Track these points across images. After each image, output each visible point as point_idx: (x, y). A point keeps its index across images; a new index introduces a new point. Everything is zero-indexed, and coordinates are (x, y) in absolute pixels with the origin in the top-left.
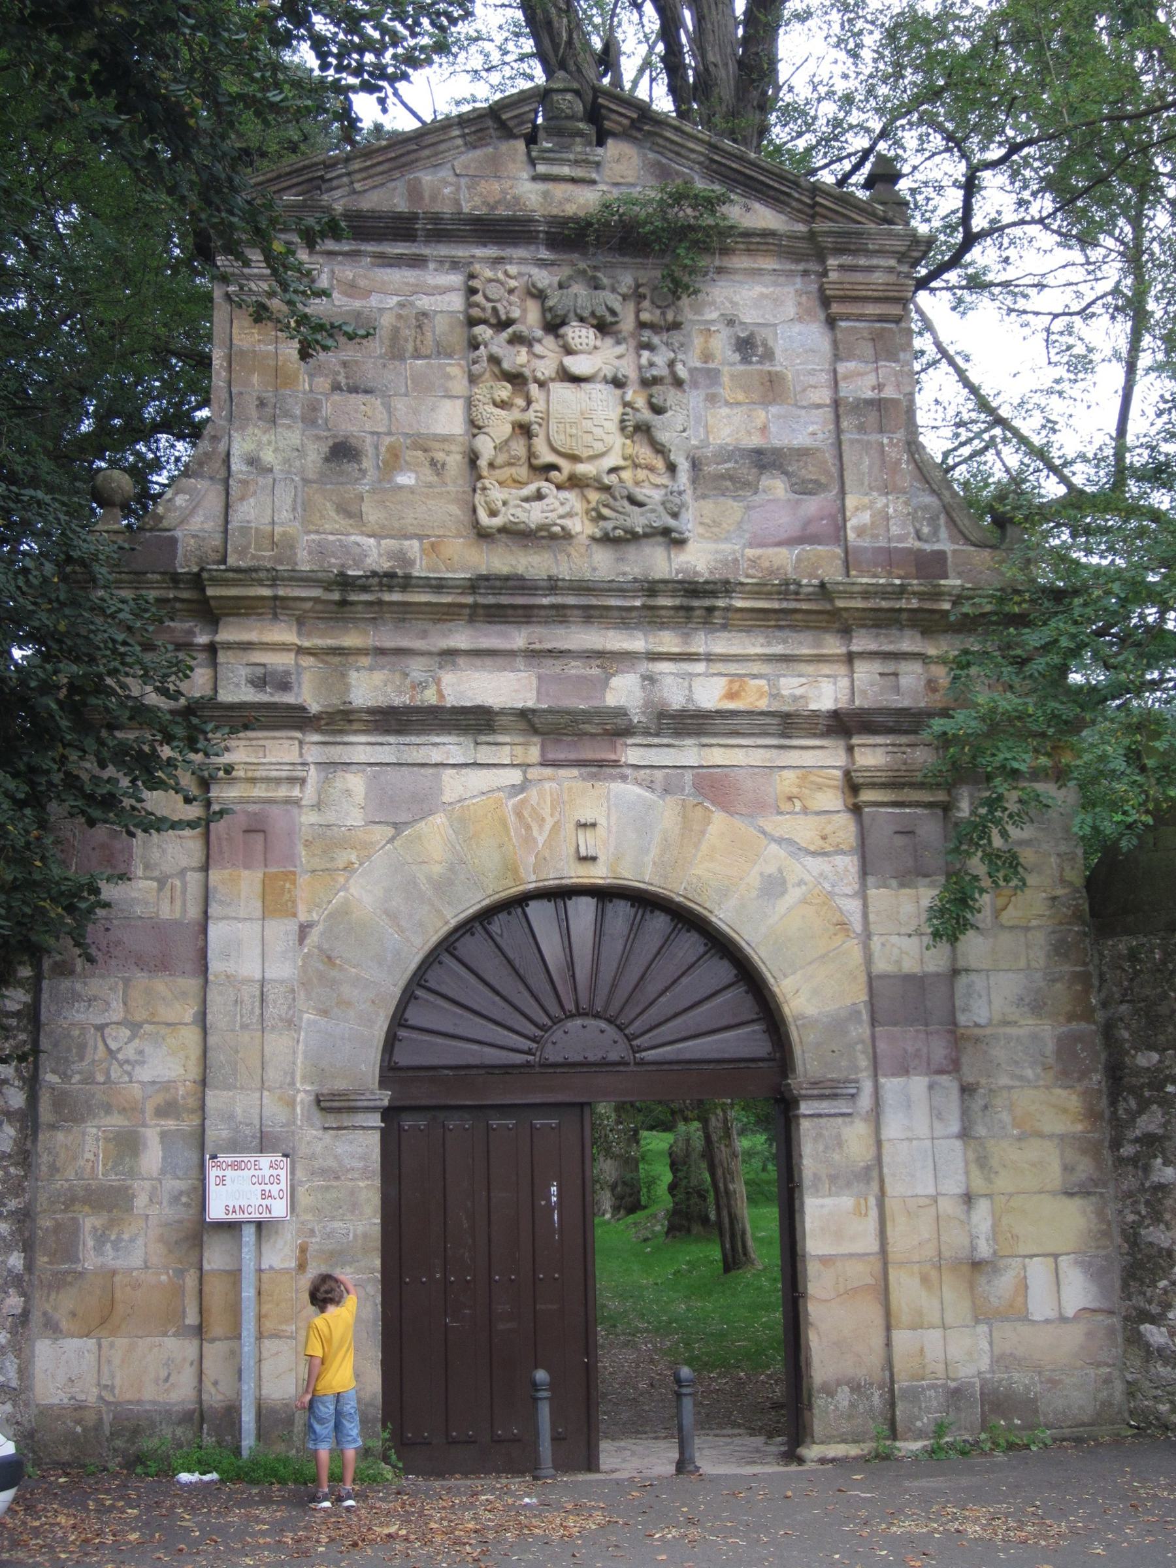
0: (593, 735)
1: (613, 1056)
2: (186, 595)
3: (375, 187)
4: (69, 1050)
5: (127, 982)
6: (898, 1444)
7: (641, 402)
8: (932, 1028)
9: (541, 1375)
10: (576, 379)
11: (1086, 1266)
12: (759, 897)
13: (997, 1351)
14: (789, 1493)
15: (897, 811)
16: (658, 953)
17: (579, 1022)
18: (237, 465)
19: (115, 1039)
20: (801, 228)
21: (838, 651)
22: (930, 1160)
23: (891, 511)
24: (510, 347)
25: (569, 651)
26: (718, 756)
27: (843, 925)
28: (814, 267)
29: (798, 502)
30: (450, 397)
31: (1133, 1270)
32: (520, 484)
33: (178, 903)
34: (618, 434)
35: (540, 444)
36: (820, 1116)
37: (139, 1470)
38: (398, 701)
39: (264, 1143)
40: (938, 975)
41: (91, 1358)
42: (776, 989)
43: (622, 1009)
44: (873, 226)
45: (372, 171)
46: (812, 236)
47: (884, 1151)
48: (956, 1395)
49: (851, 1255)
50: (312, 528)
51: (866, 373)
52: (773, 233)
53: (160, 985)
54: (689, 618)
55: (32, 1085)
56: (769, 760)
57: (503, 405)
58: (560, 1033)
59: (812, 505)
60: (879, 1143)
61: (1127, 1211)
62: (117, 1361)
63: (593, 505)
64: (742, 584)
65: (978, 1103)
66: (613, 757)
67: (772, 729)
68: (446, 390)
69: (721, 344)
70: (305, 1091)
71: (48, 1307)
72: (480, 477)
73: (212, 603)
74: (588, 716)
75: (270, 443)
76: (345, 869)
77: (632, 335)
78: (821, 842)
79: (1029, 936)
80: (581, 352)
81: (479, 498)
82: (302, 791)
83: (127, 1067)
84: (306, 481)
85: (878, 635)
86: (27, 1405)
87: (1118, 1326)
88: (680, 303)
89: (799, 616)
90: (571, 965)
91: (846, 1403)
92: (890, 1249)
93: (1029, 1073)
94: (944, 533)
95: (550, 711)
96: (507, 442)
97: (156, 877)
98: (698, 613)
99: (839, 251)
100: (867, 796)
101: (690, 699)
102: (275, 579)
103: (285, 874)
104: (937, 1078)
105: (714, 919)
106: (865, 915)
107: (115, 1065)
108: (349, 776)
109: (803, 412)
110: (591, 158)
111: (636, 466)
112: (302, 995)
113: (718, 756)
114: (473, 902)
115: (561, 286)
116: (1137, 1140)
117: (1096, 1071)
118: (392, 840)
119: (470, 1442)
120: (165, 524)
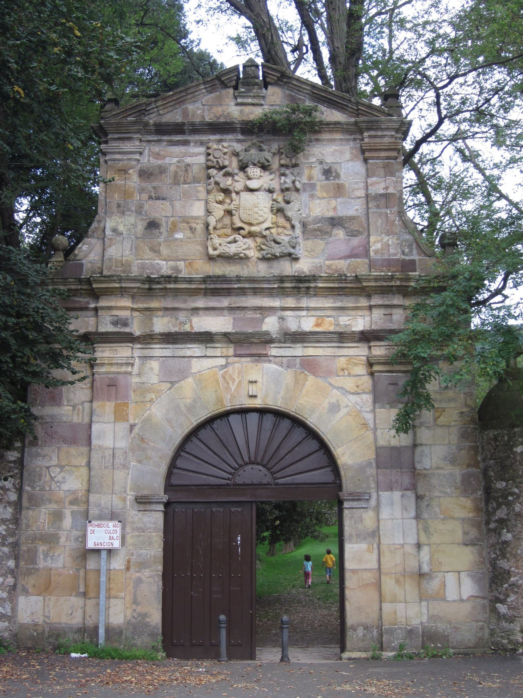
0: (256, 343)
1: (265, 481)
2: (85, 287)
3: (168, 112)
4: (35, 476)
5: (59, 448)
6: (383, 653)
7: (280, 199)
8: (403, 470)
9: (222, 617)
10: (252, 190)
11: (473, 577)
12: (328, 412)
13: (431, 614)
14: (312, 671)
15: (390, 374)
16: (286, 437)
17: (250, 466)
18: (108, 232)
19: (54, 472)
20: (353, 120)
21: (365, 305)
22: (401, 528)
23: (390, 242)
24: (224, 178)
25: (247, 307)
26: (311, 351)
27: (365, 425)
28: (358, 136)
29: (349, 240)
30: (198, 200)
31: (495, 580)
32: (227, 236)
33: (81, 415)
34: (270, 213)
35: (236, 219)
36: (353, 508)
37: (57, 651)
38: (173, 330)
39: (113, 516)
40: (406, 447)
41: (41, 604)
42: (334, 453)
43: (269, 461)
44: (383, 117)
45: (167, 106)
46: (356, 123)
47: (380, 524)
48: (410, 632)
49: (365, 569)
50: (140, 257)
51: (381, 182)
52: (339, 123)
53: (73, 450)
54: (299, 292)
55: (20, 490)
56: (334, 353)
57: (220, 203)
58: (242, 471)
59: (356, 241)
60: (378, 520)
61: (492, 553)
62: (51, 606)
63: (259, 244)
64: (321, 277)
65: (424, 504)
66: (265, 353)
67: (335, 340)
68: (197, 197)
69: (317, 172)
70: (131, 495)
71: (24, 583)
72: (210, 234)
73: (96, 290)
74: (253, 335)
75: (122, 222)
76: (150, 401)
77: (278, 170)
78: (356, 389)
79: (450, 429)
80: (254, 178)
81: (209, 243)
82: (132, 368)
83: (58, 484)
84: (137, 238)
85: (383, 297)
86: (15, 623)
87: (487, 604)
88: (299, 156)
89: (347, 290)
90: (247, 443)
91: (361, 634)
92: (382, 567)
93: (449, 490)
94: (415, 252)
95: (236, 333)
96: (222, 218)
97: (72, 403)
98: (303, 289)
99: (369, 129)
100: (376, 368)
101: (299, 327)
102: (121, 280)
103: (124, 403)
104: (405, 492)
105: (308, 422)
106: (375, 421)
107: (53, 483)
108: (152, 362)
109: (353, 201)
110: (260, 95)
111: (278, 227)
112: (130, 454)
113: (311, 351)
114: (203, 415)
115: (246, 151)
116: (496, 521)
117: (480, 490)
118: (170, 388)
119: (201, 645)
120: (78, 258)
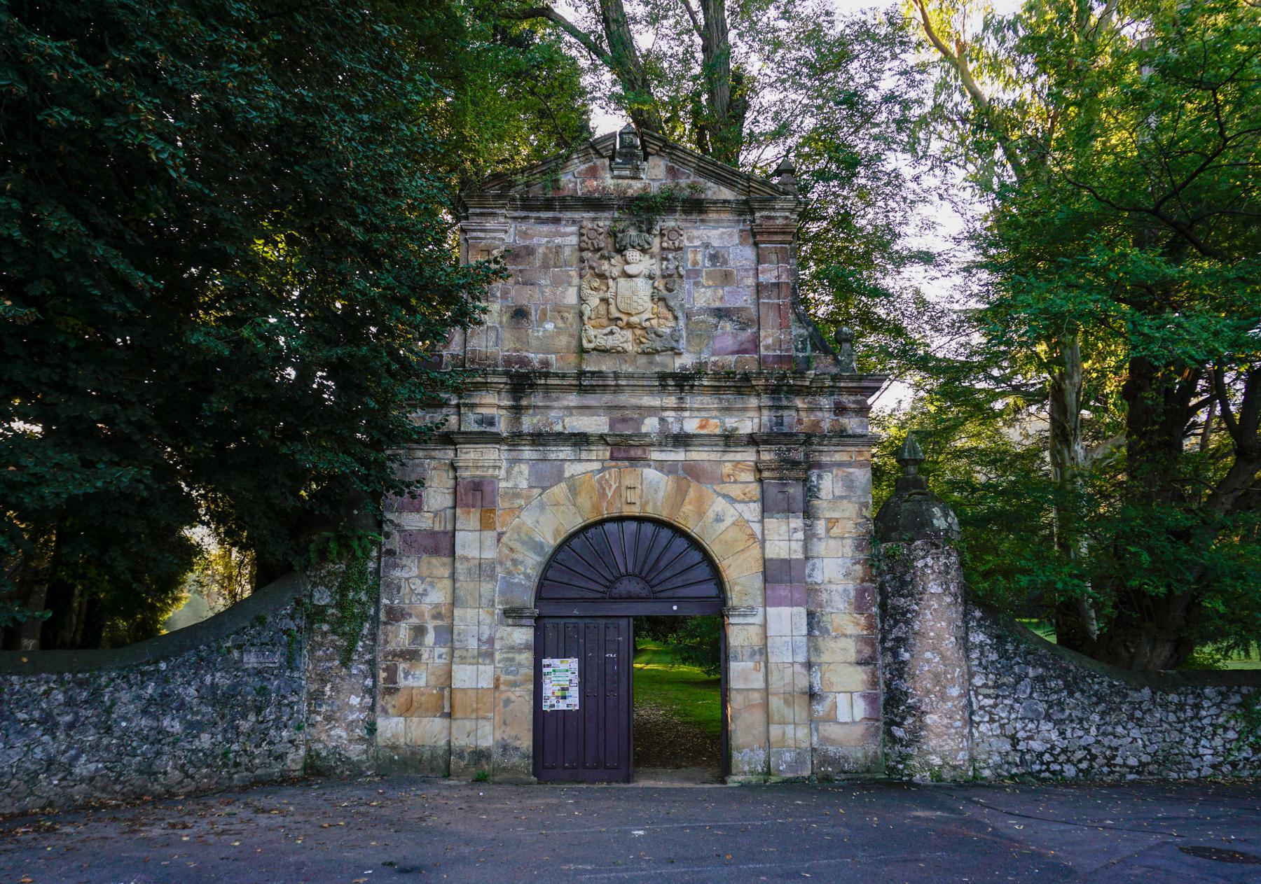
5: (420, 558)
7: (661, 287)
28: (748, 217)
32: (603, 327)
35: (613, 309)
41: (401, 726)
52: (729, 202)
53: (435, 561)
57: (595, 289)
60: (766, 637)
101: (681, 429)
